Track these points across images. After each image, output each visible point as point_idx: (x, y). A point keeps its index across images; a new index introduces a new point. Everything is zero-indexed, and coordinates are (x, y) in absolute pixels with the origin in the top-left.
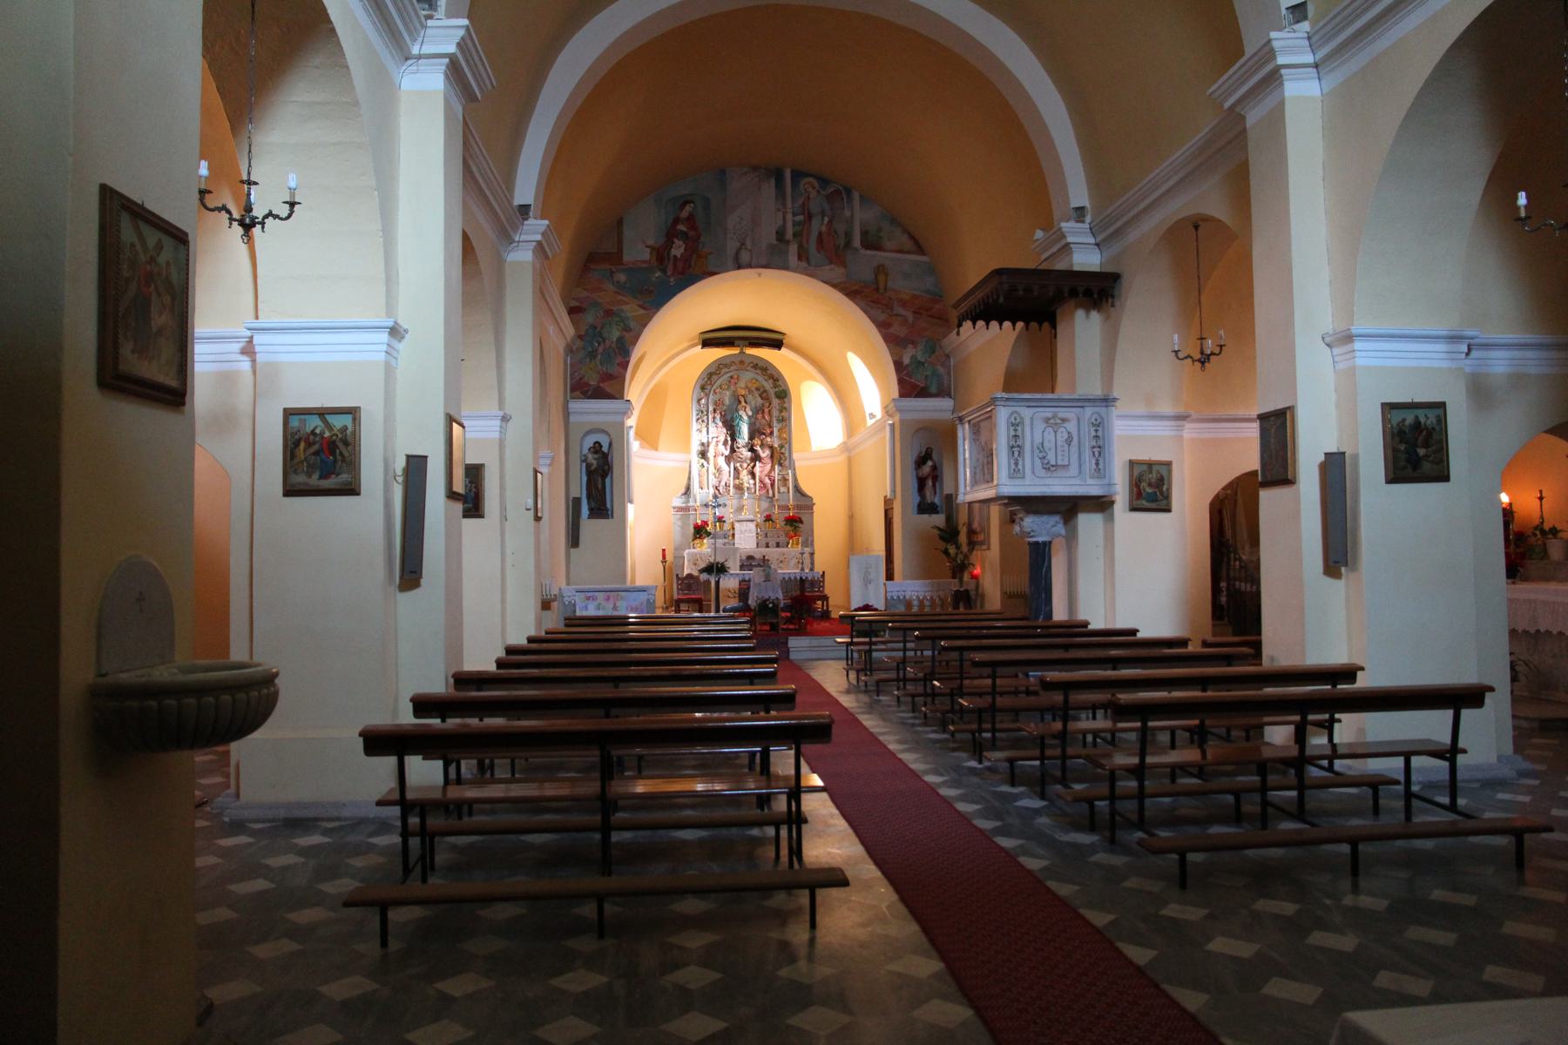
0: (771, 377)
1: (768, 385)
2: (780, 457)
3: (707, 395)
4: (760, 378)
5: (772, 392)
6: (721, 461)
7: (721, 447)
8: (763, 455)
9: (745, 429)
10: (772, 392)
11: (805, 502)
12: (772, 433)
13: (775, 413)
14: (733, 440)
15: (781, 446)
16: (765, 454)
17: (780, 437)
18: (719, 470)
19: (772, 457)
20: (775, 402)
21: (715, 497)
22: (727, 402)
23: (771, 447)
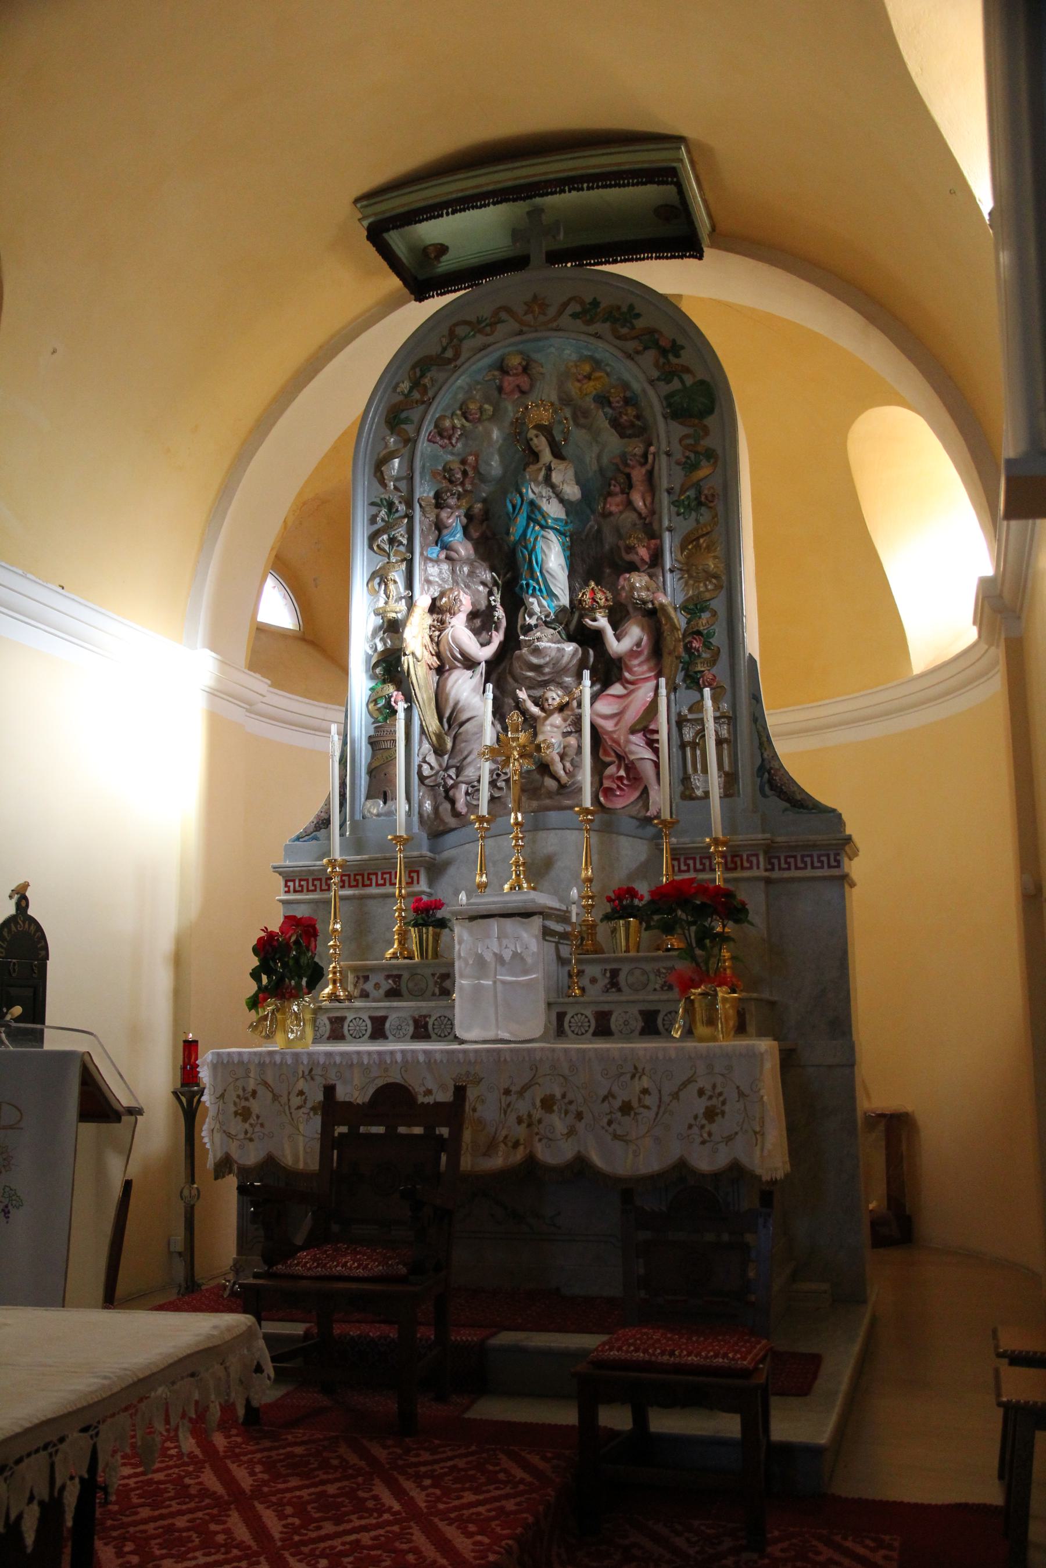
0: (650, 339)
1: (635, 374)
2: (698, 649)
3: (410, 442)
4: (603, 350)
5: (654, 403)
6: (469, 691)
7: (459, 631)
8: (616, 646)
9: (553, 559)
10: (654, 403)
11: (799, 837)
12: (656, 559)
13: (668, 476)
14: (514, 603)
15: (694, 607)
16: (624, 642)
17: (688, 570)
18: (451, 719)
19: (657, 651)
20: (668, 435)
21: (437, 830)
22: (495, 466)
23: (653, 616)
